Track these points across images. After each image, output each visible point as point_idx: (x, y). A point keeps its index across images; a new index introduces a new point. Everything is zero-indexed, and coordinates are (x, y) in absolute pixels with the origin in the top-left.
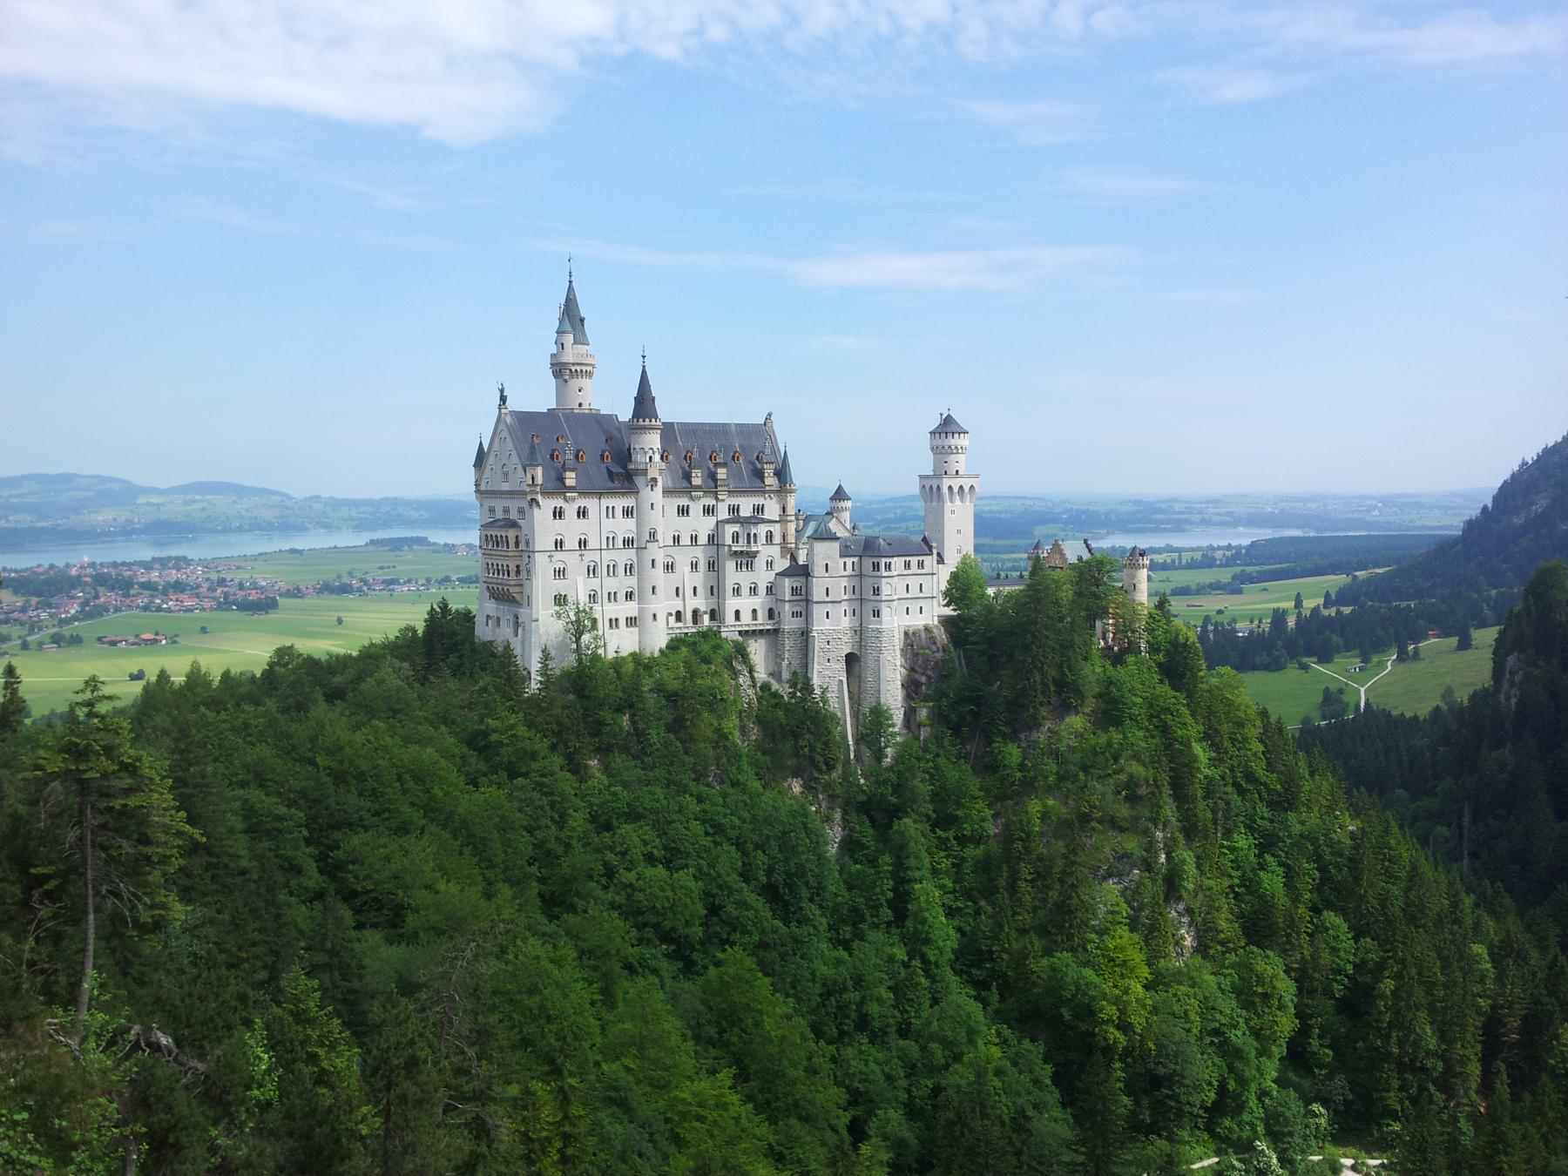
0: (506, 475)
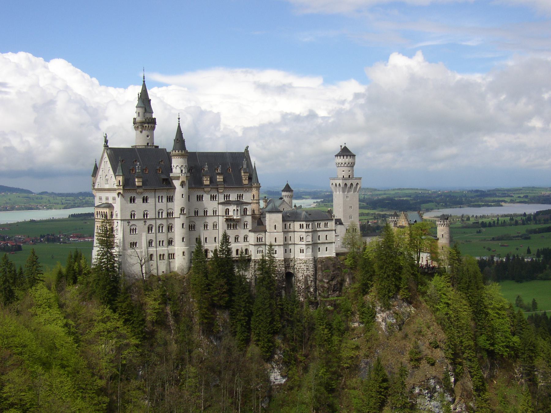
0: (107, 180)
